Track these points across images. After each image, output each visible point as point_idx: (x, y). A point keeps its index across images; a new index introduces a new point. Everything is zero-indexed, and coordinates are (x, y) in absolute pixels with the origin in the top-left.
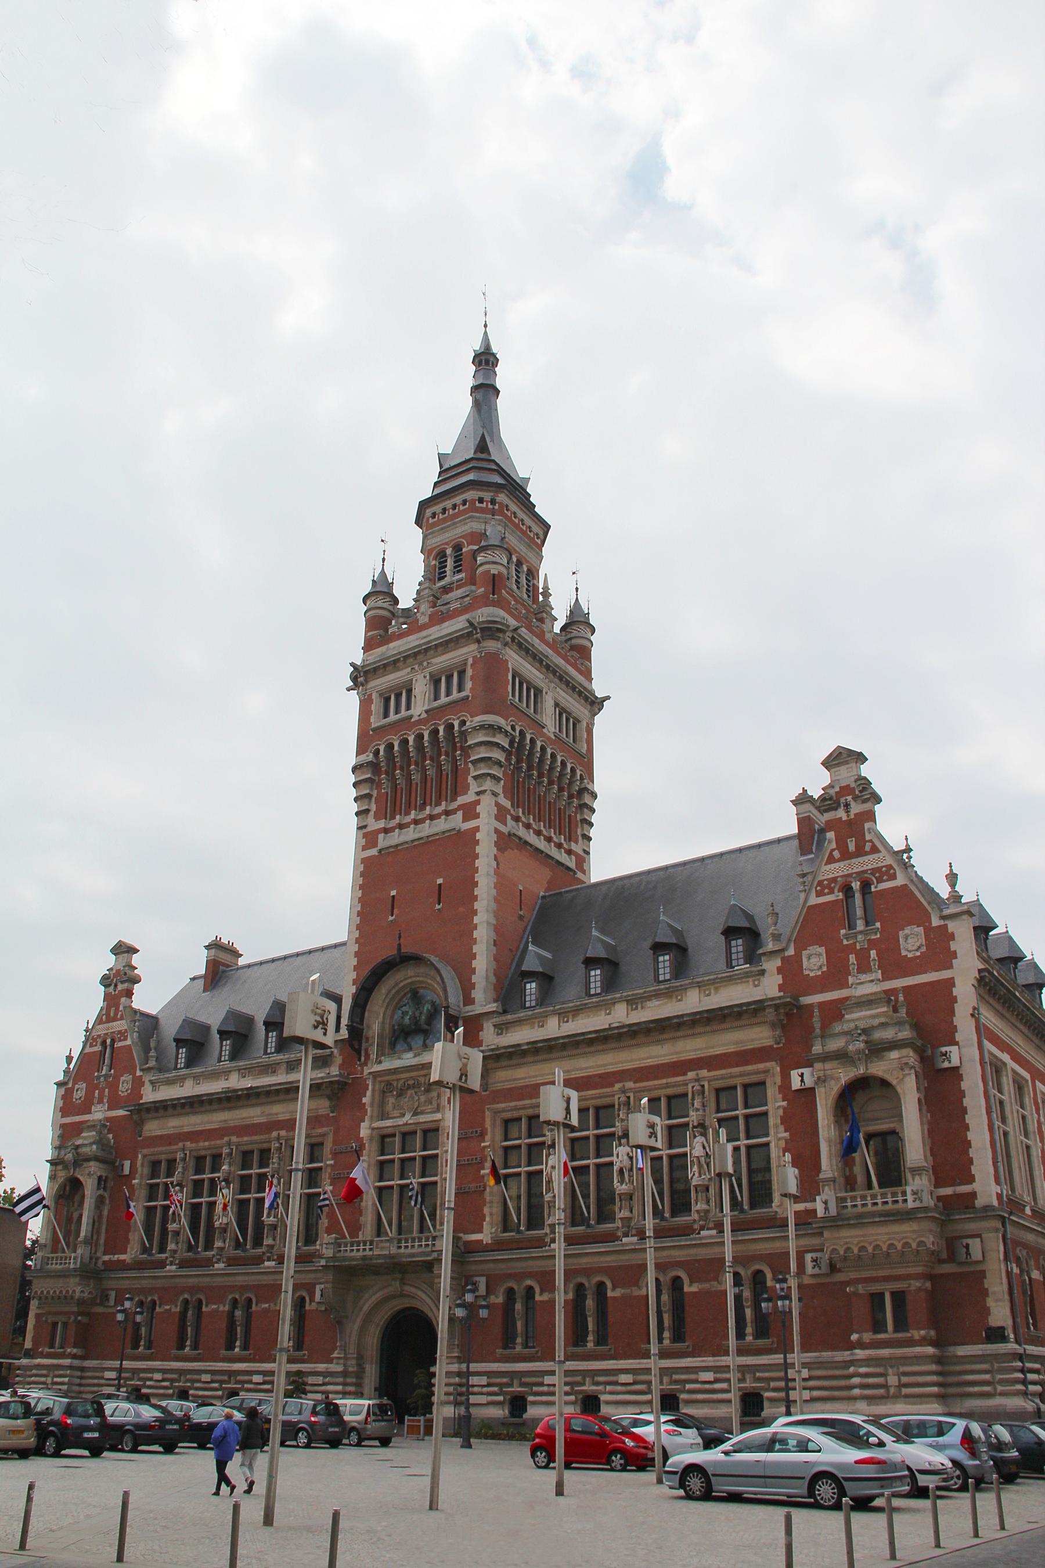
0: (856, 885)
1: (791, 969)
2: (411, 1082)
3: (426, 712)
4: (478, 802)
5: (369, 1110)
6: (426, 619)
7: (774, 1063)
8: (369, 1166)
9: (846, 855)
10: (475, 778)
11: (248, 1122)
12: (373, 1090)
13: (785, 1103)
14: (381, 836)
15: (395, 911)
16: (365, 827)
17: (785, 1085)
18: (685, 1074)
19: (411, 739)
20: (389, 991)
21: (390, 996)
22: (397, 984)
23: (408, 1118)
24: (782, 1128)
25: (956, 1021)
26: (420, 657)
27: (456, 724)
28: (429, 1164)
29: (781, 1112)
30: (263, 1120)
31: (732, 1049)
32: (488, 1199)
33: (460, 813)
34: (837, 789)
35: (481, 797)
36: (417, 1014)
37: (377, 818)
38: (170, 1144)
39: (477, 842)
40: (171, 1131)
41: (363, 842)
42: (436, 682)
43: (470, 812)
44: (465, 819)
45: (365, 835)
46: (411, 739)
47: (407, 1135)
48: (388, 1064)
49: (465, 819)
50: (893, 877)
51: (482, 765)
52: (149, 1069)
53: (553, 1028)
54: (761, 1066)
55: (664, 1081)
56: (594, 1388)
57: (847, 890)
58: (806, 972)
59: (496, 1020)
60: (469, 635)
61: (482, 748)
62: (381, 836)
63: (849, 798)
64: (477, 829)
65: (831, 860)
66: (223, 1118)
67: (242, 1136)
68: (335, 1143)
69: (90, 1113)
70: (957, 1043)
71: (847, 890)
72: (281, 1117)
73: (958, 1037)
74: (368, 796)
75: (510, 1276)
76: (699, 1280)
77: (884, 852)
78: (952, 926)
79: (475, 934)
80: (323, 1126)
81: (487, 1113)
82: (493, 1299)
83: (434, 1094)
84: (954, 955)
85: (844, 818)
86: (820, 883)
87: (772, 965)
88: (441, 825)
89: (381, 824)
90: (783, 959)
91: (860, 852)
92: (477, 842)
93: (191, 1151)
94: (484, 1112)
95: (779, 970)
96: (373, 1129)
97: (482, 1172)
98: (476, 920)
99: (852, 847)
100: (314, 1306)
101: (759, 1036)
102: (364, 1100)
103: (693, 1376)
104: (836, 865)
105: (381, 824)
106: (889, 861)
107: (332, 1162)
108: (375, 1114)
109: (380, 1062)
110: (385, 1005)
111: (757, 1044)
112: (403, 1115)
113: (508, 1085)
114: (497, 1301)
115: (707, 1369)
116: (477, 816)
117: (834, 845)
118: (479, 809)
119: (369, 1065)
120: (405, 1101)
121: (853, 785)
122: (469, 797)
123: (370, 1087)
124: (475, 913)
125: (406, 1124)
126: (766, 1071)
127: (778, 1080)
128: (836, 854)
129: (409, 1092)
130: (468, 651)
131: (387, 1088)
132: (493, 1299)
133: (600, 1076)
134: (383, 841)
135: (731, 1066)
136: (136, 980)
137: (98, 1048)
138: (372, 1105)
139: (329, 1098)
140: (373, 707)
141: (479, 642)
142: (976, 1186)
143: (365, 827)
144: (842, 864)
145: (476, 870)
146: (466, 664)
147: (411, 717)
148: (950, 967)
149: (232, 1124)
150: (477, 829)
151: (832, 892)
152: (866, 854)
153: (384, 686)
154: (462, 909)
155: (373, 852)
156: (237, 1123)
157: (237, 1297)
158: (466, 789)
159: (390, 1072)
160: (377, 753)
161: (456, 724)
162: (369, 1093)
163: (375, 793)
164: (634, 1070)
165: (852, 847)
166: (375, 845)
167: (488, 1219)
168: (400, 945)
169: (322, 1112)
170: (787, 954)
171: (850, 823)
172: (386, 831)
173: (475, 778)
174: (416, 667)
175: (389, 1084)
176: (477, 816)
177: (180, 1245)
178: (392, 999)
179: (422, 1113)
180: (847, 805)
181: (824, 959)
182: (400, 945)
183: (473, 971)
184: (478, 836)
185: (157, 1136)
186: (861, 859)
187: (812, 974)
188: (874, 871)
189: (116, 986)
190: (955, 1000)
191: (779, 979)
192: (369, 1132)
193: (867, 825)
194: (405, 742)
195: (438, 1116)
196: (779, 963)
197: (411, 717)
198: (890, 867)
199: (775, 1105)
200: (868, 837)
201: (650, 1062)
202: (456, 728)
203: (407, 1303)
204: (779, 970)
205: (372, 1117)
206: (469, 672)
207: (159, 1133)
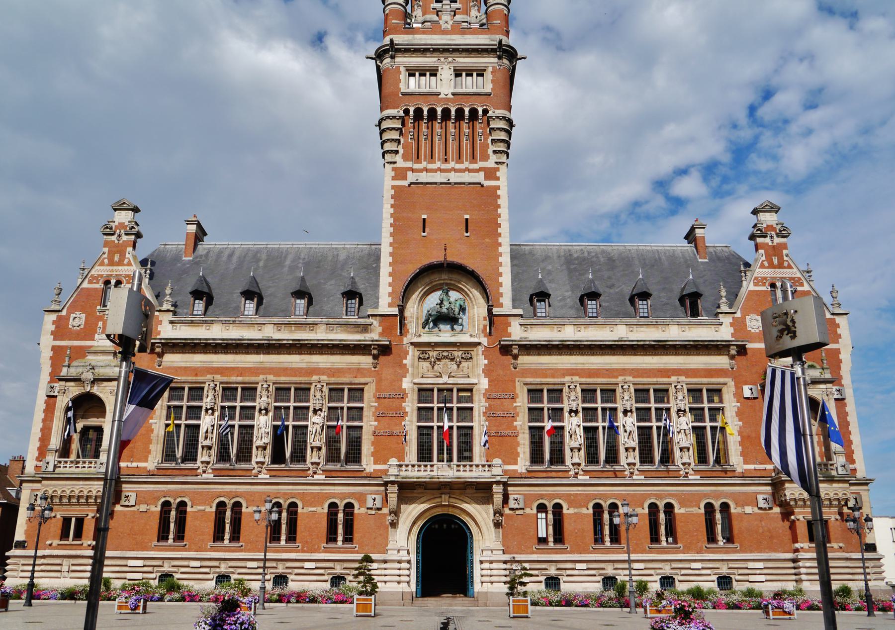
0: (779, 284)
1: (739, 325)
2: (445, 354)
3: (453, 94)
4: (498, 169)
5: (410, 370)
6: (449, 27)
7: (730, 380)
8: (412, 410)
9: (771, 266)
10: (495, 152)
11: (286, 365)
12: (414, 356)
13: (739, 404)
14: (409, 173)
15: (426, 229)
16: (395, 163)
17: (739, 394)
18: (669, 377)
19: (439, 110)
23: (445, 379)
24: (737, 419)
25: (842, 373)
26: (446, 55)
27: (480, 110)
28: (466, 412)
29: (736, 409)
30: (304, 365)
31: (702, 367)
32: (521, 442)
33: (482, 174)
34: (764, 225)
35: (500, 166)
37: (405, 158)
38: (196, 375)
39: (499, 197)
40: (199, 365)
41: (393, 174)
42: (458, 74)
43: (491, 174)
44: (487, 178)
45: (394, 169)
46: (439, 110)
47: (445, 392)
48: (425, 338)
49: (487, 178)
50: (802, 285)
51: (502, 144)
52: (168, 311)
53: (569, 333)
54: (722, 380)
55: (655, 380)
56: (615, 572)
57: (773, 285)
58: (749, 329)
59: (522, 321)
60: (493, 51)
61: (503, 133)
62: (409, 173)
63: (773, 233)
64: (498, 188)
65: (762, 266)
66: (258, 360)
67: (279, 376)
68: (377, 390)
69: (93, 340)
70: (843, 386)
71: (773, 285)
72: (321, 366)
73: (843, 382)
74: (398, 141)
75: (541, 496)
76: (686, 506)
77: (795, 270)
78: (838, 319)
79: (501, 259)
80: (365, 376)
81: (517, 383)
82: (528, 511)
83: (465, 364)
84: (840, 336)
85: (770, 243)
86: (756, 278)
87: (726, 320)
88: (467, 178)
89: (409, 164)
90: (733, 318)
91: (780, 266)
92: (499, 197)
93: (221, 383)
94: (514, 382)
95: (732, 325)
97: (515, 423)
98: (500, 250)
99: (776, 261)
100: (363, 510)
101: (721, 361)
102: (405, 362)
103: (687, 566)
104: (764, 270)
105: (409, 164)
106: (799, 275)
107: (376, 404)
108: (415, 373)
109: (420, 336)
111: (719, 366)
113: (533, 366)
114: (531, 512)
115: (695, 561)
116: (498, 179)
117: (764, 258)
118: (498, 174)
119: (409, 336)
120: (439, 367)
121: (775, 226)
122: (490, 163)
123: (411, 353)
124: (500, 245)
125: (446, 384)
126: (725, 384)
127: (733, 389)
128: (766, 264)
129: (444, 361)
130: (490, 62)
132: (528, 511)
133: (607, 370)
134: (411, 177)
135: (701, 377)
136: (138, 235)
137: (100, 285)
138: (413, 366)
139: (375, 357)
140: (402, 77)
141: (500, 58)
142: (856, 466)
143: (395, 163)
144: (770, 270)
145: (499, 216)
146: (485, 70)
147: (439, 94)
148: (838, 342)
149: (268, 365)
150: (498, 188)
151: (764, 285)
152: (785, 268)
153: (412, 65)
154: (487, 240)
155: (405, 183)
156: (274, 365)
157: (281, 501)
158: (485, 158)
159: (429, 344)
160: (407, 112)
161: (480, 110)
162: (409, 357)
163: (402, 141)
164: (633, 369)
165: (776, 261)
166: (405, 178)
167: (521, 455)
169: (363, 366)
170: (736, 315)
171: (774, 247)
172: (413, 170)
173: (495, 152)
174: (442, 59)
176: (498, 179)
177: (212, 457)
180: (771, 237)
181: (760, 324)
183: (501, 285)
184: (499, 192)
185: (180, 368)
186: (782, 270)
187: (753, 331)
188: (791, 279)
189: (120, 236)
190: (840, 361)
191: (732, 330)
192: (411, 385)
193: (785, 252)
194: (432, 111)
196: (731, 321)
197: (439, 94)
198: (799, 279)
199: (730, 404)
200: (785, 258)
201: (645, 366)
202: (480, 113)
203: (444, 511)
204: (732, 325)
206: (488, 75)
207: (183, 365)
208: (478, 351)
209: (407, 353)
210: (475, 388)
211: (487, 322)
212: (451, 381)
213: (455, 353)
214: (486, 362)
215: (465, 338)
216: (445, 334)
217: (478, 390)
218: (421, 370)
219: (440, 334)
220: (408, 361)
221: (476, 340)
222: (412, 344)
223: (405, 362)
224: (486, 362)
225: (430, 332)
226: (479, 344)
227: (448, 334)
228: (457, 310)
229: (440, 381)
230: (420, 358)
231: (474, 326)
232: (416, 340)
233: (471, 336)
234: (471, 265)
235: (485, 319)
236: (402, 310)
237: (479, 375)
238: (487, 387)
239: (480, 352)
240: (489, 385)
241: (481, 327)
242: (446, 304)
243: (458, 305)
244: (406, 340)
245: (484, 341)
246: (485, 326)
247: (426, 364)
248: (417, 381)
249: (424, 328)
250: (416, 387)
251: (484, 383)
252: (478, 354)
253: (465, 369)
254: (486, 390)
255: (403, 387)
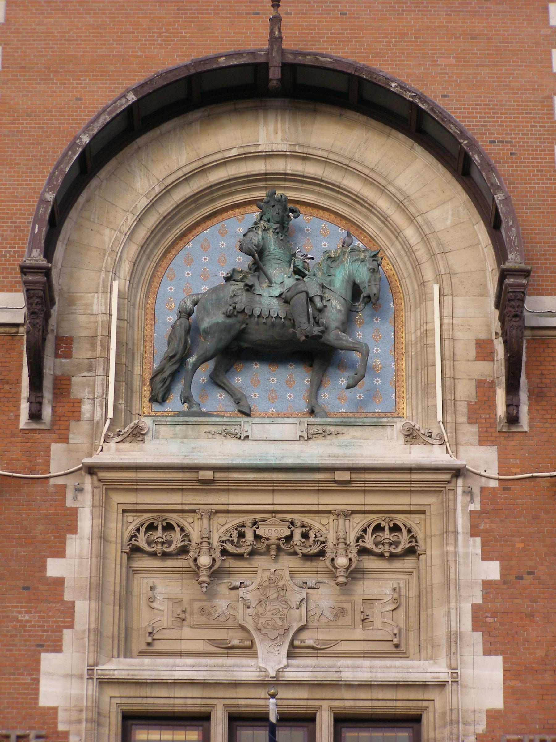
5: (83, 609)
12: (102, 537)
20: (168, 191)
21: (165, 208)
22: (203, 170)
23: (270, 660)
36: (314, 290)
48: (166, 445)
83: (381, 585)
96: (105, 682)
102: (54, 568)
108: (110, 627)
109: (137, 434)
110: (142, 234)
112: (249, 649)
119: (79, 436)
123: (86, 522)
131: (154, 540)
138: (98, 590)
162: (79, 545)
168: (276, 21)
175: (159, 524)
178: (168, 221)
179: (315, 650)
182: (276, 21)
192: (85, 690)
195: (435, 670)
205: (97, 634)
208: (448, 513)
209: (68, 522)
210: (437, 706)
211: (497, 368)
212: (302, 670)
213: (328, 529)
214: (492, 571)
215: (383, 448)
216: (272, 427)
217: (455, 719)
218: (143, 619)
219: (253, 427)
220: (71, 566)
221: (437, 456)
222: (91, 470)
223: (54, 568)
224: (492, 571)
225: (193, 413)
226: (458, 472)
227: (287, 428)
228: (335, 307)
229: (245, 669)
230: (136, 550)
231: (427, 389)
232: (113, 453)
233: (411, 436)
234: (403, 71)
235: (483, 350)
236: (42, 296)
237: (454, 640)
238: (497, 701)
239: (462, 522)
240: (510, 693)
241: (465, 391)
242: (280, 277)
243: (339, 279)
244: (60, 460)
245: (483, 460)
246: (485, 388)
247: (163, 588)
248: (117, 667)
249: (159, 398)
250: (113, 703)
251: (485, 682)
252: (448, 533)
253: (379, 615)
254: (492, 716)
255: (44, 701)
